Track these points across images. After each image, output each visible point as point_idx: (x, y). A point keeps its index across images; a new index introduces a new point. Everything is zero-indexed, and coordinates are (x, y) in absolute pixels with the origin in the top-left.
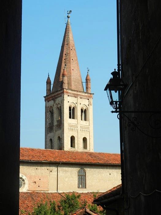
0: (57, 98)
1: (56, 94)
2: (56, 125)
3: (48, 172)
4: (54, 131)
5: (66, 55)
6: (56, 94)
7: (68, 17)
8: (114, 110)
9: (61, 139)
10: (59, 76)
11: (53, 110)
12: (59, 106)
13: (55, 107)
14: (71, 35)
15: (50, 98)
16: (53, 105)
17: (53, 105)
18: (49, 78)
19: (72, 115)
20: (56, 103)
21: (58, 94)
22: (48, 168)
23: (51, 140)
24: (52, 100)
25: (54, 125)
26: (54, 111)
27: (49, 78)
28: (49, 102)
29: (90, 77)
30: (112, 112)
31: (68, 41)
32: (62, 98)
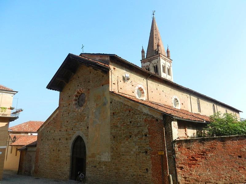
1: (153, 57)
3: (187, 98)
6: (153, 57)
7: (153, 14)
10: (153, 47)
12: (155, 65)
13: (151, 65)
14: (157, 24)
16: (149, 65)
18: (143, 50)
19: (164, 72)
21: (154, 58)
22: (187, 95)
24: (149, 61)
27: (143, 50)
28: (145, 63)
29: (170, 50)
31: (156, 27)
32: (158, 59)
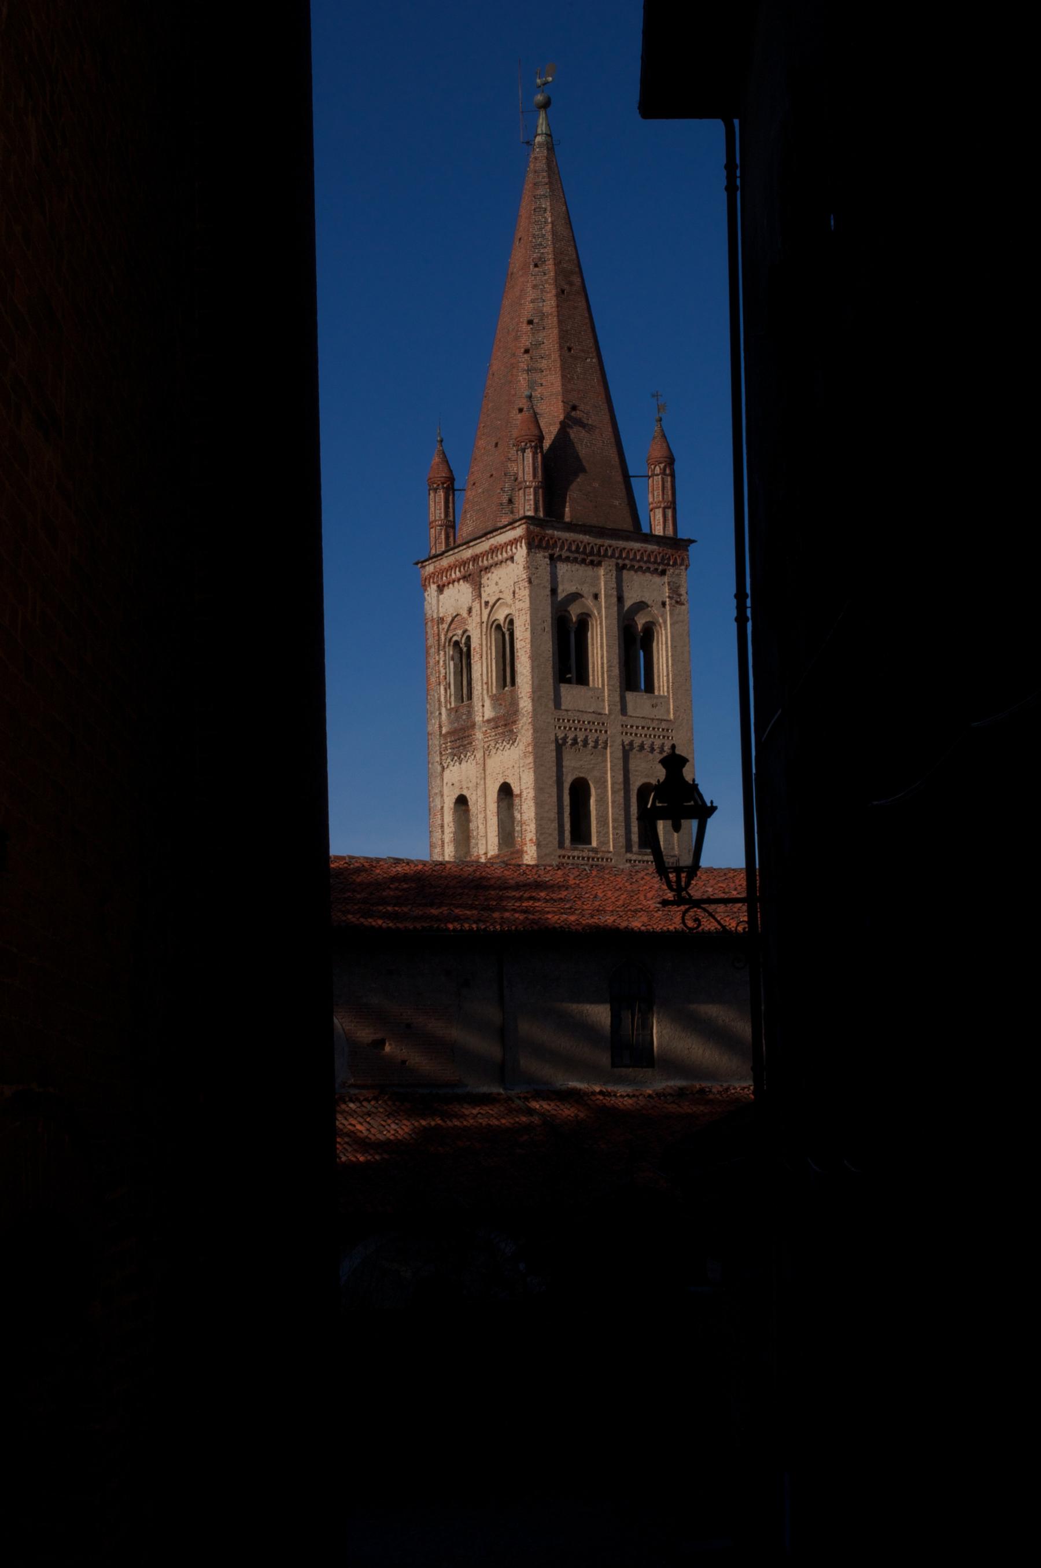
0: (487, 569)
2: (489, 721)
4: (479, 755)
5: (530, 322)
6: (484, 546)
8: (670, 895)
9: (520, 796)
11: (469, 638)
15: (451, 568)
16: (470, 610)
17: (470, 610)
20: (485, 597)
21: (494, 550)
23: (462, 801)
24: (465, 578)
25: (478, 719)
26: (473, 646)
30: (665, 903)
